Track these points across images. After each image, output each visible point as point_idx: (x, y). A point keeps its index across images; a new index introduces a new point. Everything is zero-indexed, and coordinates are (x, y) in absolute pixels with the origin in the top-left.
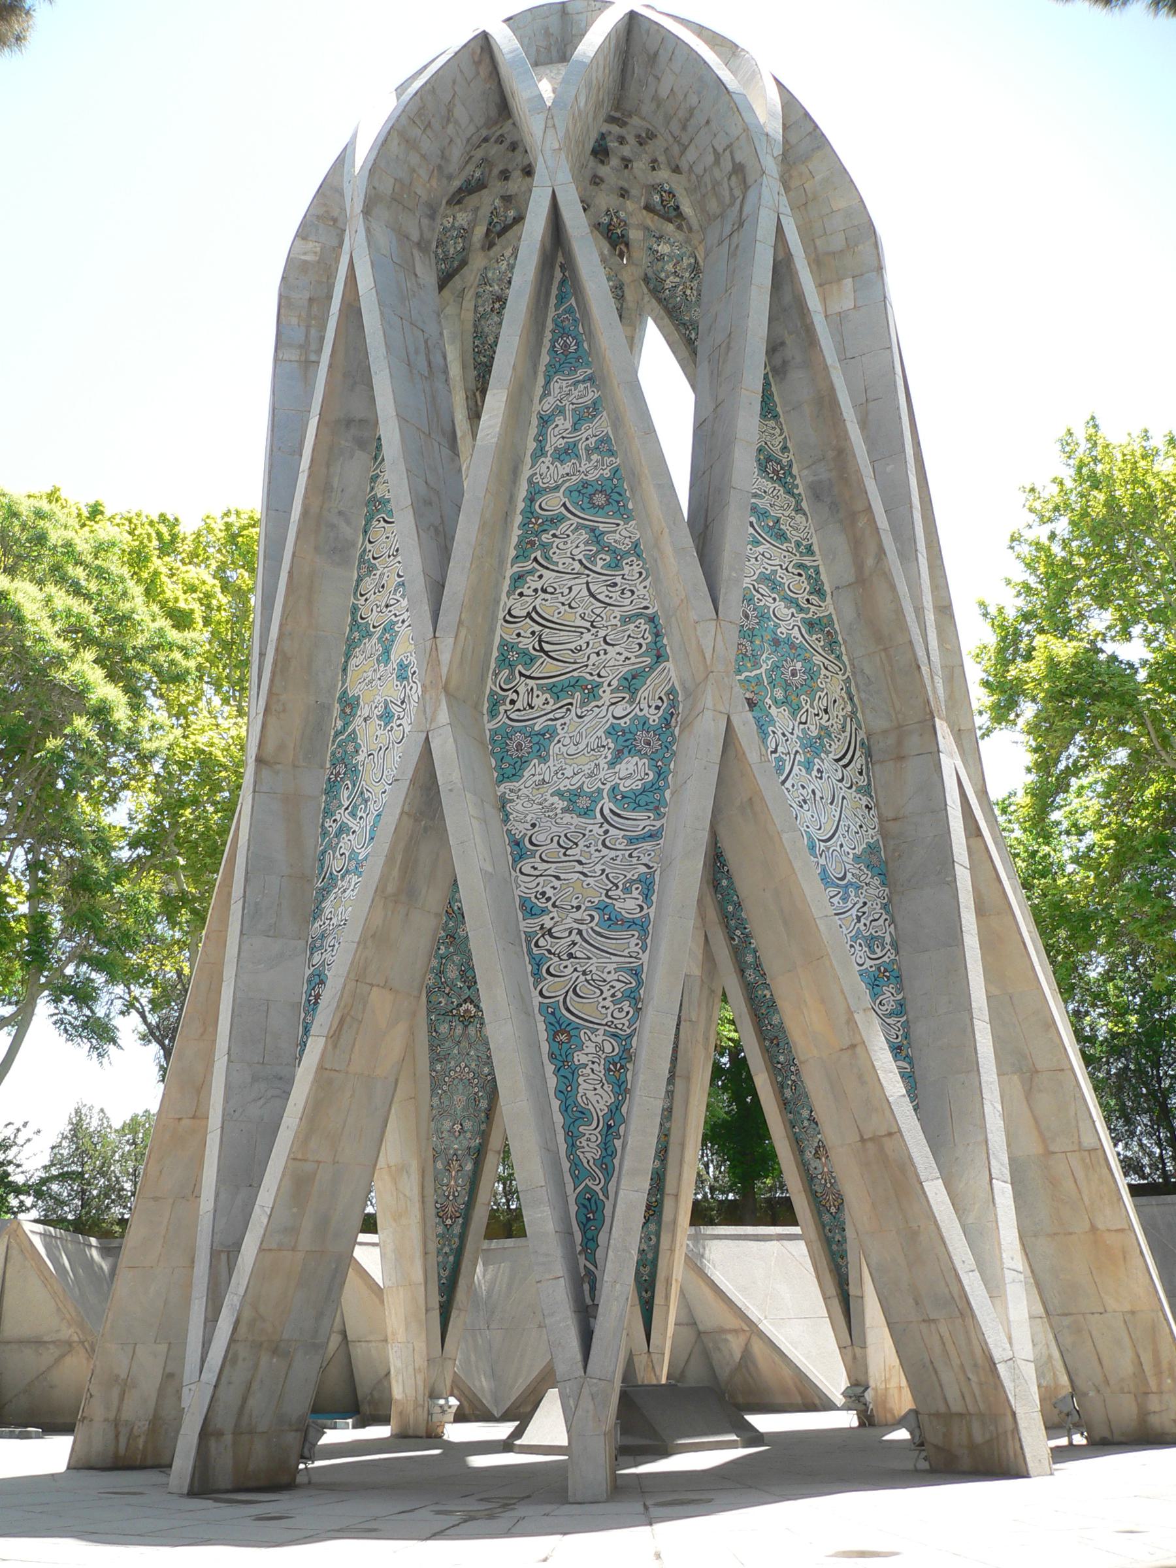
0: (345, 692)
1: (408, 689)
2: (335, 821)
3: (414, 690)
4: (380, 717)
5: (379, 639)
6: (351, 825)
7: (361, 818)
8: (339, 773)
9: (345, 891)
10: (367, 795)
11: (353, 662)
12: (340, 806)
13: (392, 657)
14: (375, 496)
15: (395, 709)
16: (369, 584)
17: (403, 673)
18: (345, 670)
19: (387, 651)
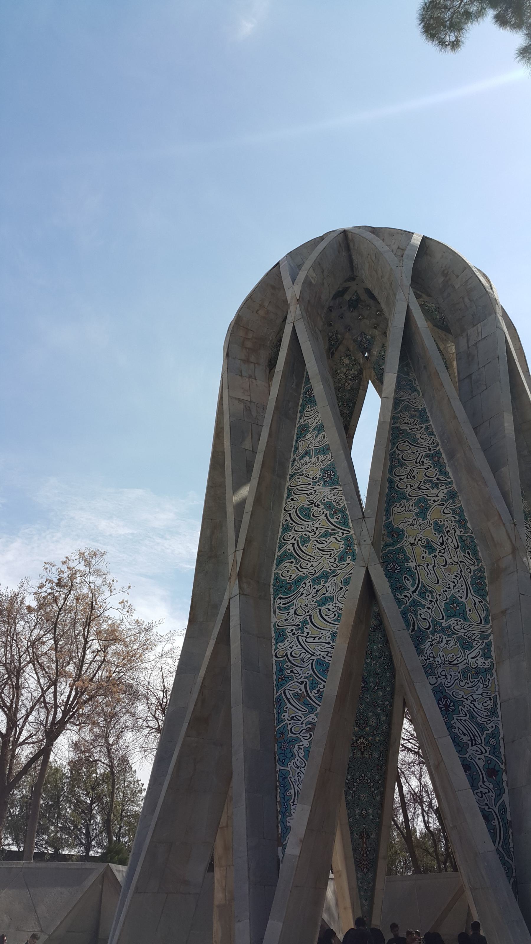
0: (390, 523)
1: (445, 539)
2: (405, 596)
3: (450, 539)
4: (425, 547)
5: (416, 504)
6: (423, 603)
7: (431, 601)
8: (394, 569)
9: (438, 643)
10: (430, 589)
11: (393, 510)
12: (406, 588)
13: (428, 517)
14: (398, 427)
15: (438, 548)
16: (400, 470)
17: (438, 528)
18: (388, 511)
19: (423, 513)
